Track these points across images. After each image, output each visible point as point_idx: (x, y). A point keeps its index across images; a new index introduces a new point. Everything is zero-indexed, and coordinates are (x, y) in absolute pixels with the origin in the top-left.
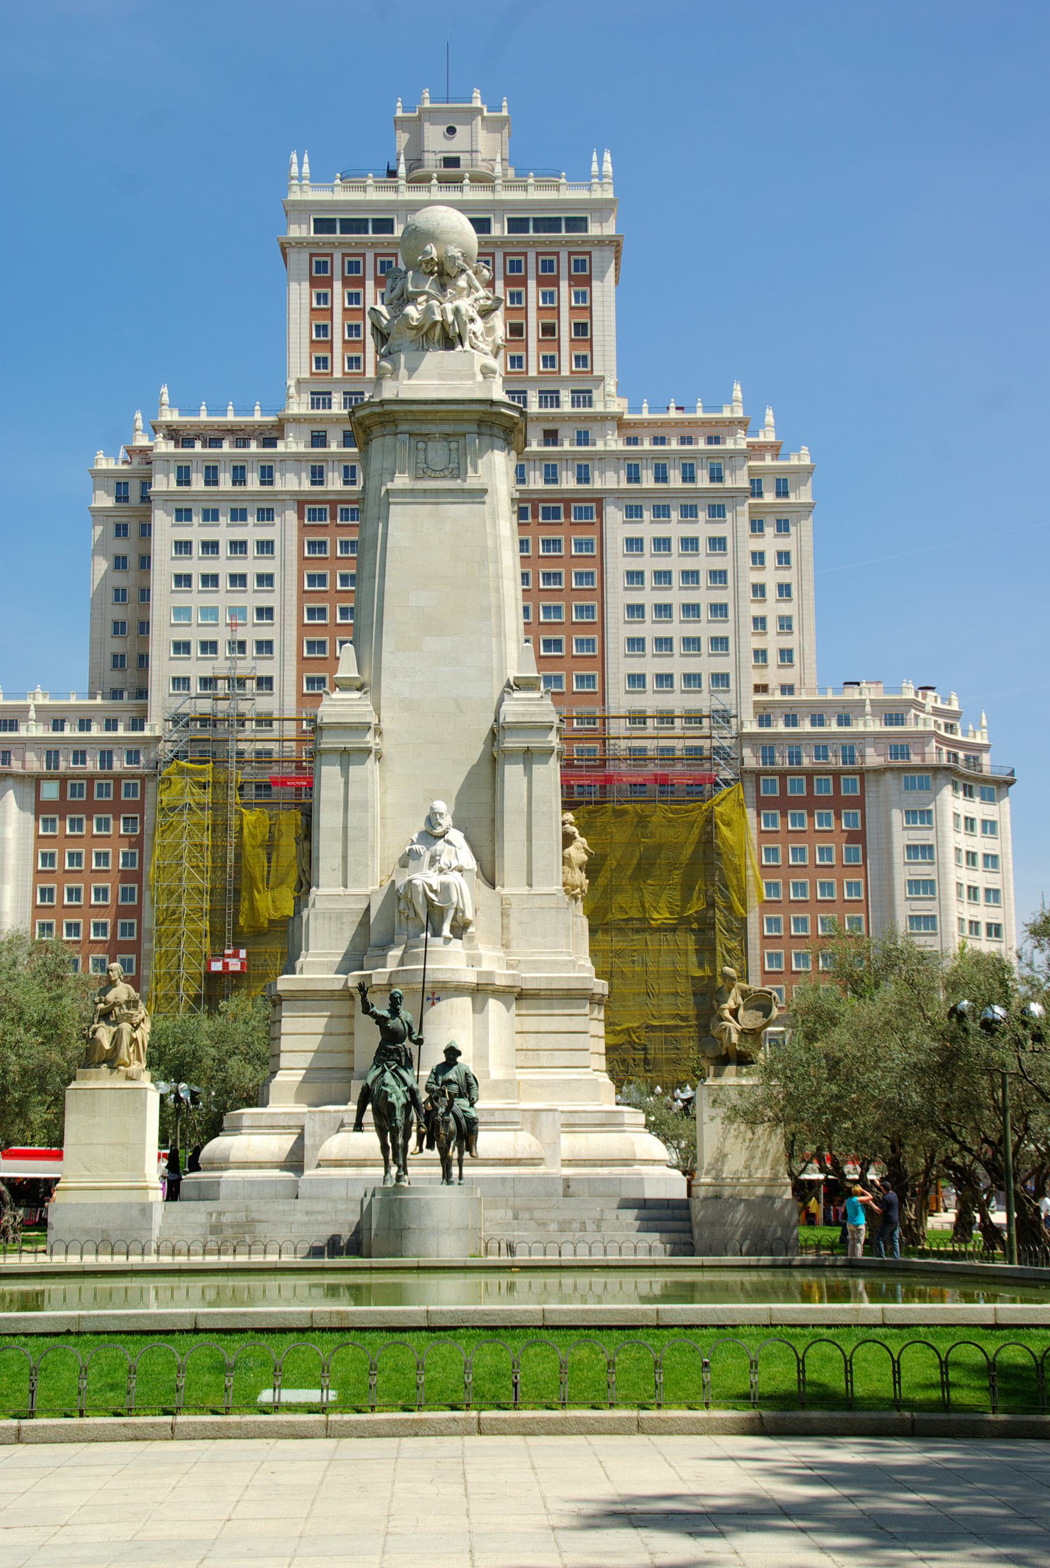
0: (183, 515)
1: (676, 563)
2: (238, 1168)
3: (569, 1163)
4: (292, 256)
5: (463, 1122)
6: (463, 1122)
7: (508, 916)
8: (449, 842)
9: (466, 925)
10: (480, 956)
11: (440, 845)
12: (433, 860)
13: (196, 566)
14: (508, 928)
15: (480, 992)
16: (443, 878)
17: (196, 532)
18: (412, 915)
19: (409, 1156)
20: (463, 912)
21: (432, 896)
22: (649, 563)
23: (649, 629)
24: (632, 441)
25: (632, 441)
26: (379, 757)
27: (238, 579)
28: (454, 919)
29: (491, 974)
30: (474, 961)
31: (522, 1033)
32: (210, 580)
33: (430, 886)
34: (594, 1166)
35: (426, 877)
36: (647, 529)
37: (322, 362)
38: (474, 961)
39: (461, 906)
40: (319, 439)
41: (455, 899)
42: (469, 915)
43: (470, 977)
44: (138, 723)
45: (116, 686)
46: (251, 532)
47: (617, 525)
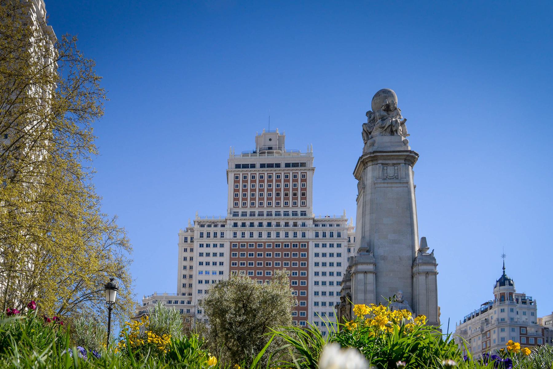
0: (202, 246)
1: (328, 260)
4: (230, 174)
13: (204, 259)
17: (205, 250)
22: (321, 260)
23: (320, 279)
24: (316, 225)
25: (316, 225)
27: (215, 264)
32: (208, 264)
36: (320, 250)
37: (236, 204)
40: (235, 225)
44: (189, 302)
45: (184, 292)
46: (218, 250)
47: (312, 250)
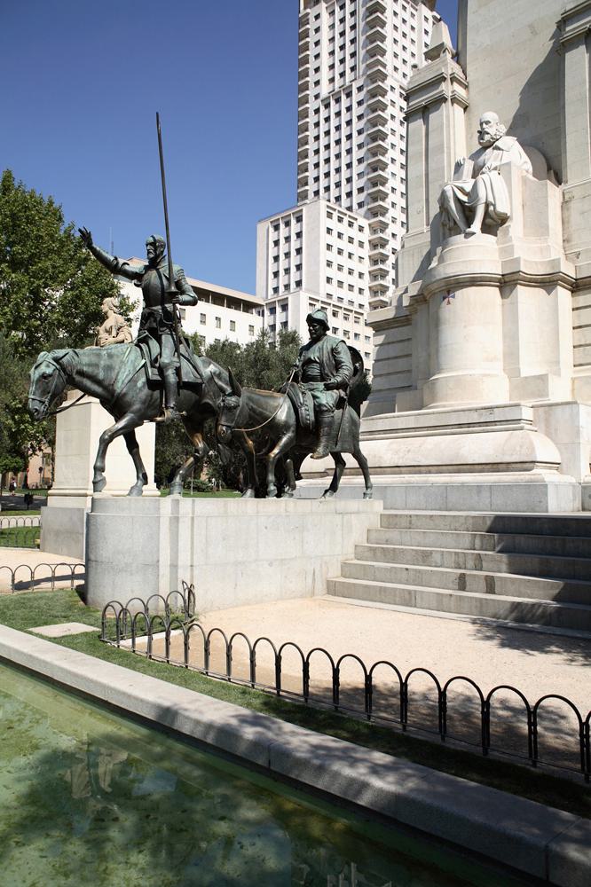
5: (308, 413)
7: (568, 209)
8: (498, 148)
9: (504, 219)
10: (513, 246)
14: (568, 222)
18: (452, 224)
20: (494, 206)
21: (465, 198)
26: (454, 100)
28: (487, 213)
29: (517, 261)
30: (507, 250)
31: (580, 327)
33: (462, 190)
38: (507, 250)
42: (502, 208)
43: (495, 268)
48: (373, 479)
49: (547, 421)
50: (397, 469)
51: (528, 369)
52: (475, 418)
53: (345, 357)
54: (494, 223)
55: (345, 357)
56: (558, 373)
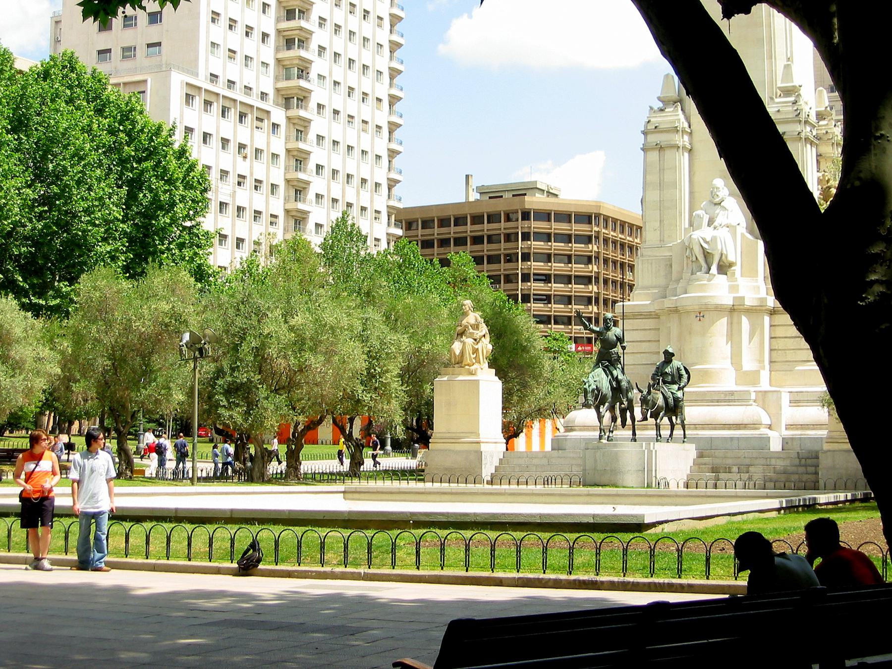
2: (580, 430)
3: (789, 427)
5: (671, 401)
6: (671, 401)
8: (725, 209)
9: (731, 265)
11: (718, 210)
12: (711, 222)
15: (734, 310)
16: (715, 233)
18: (694, 259)
19: (636, 423)
29: (743, 298)
30: (733, 288)
33: (704, 240)
34: (715, 429)
35: (704, 233)
38: (733, 288)
39: (724, 252)
41: (719, 247)
42: (731, 258)
43: (727, 300)
48: (687, 432)
49: (763, 401)
50: (696, 426)
51: (748, 364)
52: (722, 397)
53: (683, 372)
54: (724, 268)
55: (683, 372)
56: (764, 369)
